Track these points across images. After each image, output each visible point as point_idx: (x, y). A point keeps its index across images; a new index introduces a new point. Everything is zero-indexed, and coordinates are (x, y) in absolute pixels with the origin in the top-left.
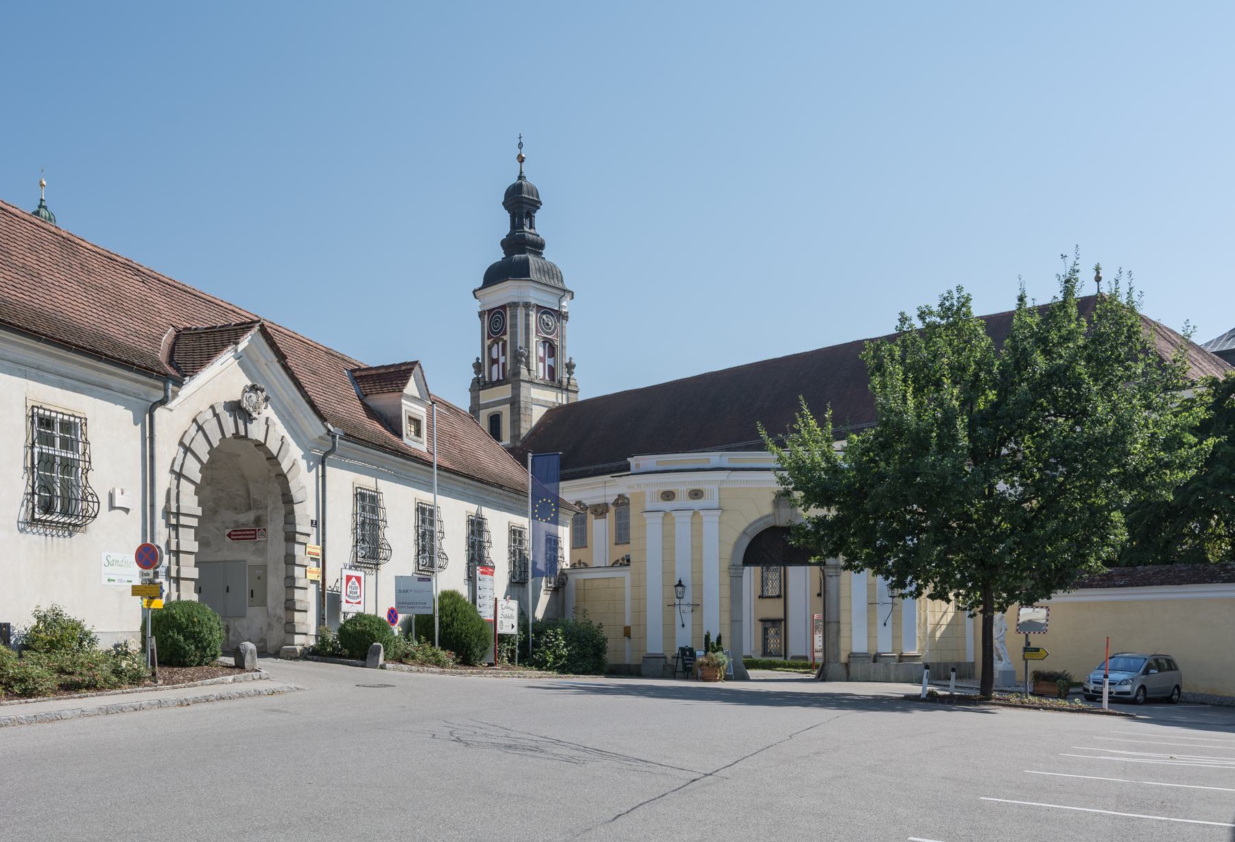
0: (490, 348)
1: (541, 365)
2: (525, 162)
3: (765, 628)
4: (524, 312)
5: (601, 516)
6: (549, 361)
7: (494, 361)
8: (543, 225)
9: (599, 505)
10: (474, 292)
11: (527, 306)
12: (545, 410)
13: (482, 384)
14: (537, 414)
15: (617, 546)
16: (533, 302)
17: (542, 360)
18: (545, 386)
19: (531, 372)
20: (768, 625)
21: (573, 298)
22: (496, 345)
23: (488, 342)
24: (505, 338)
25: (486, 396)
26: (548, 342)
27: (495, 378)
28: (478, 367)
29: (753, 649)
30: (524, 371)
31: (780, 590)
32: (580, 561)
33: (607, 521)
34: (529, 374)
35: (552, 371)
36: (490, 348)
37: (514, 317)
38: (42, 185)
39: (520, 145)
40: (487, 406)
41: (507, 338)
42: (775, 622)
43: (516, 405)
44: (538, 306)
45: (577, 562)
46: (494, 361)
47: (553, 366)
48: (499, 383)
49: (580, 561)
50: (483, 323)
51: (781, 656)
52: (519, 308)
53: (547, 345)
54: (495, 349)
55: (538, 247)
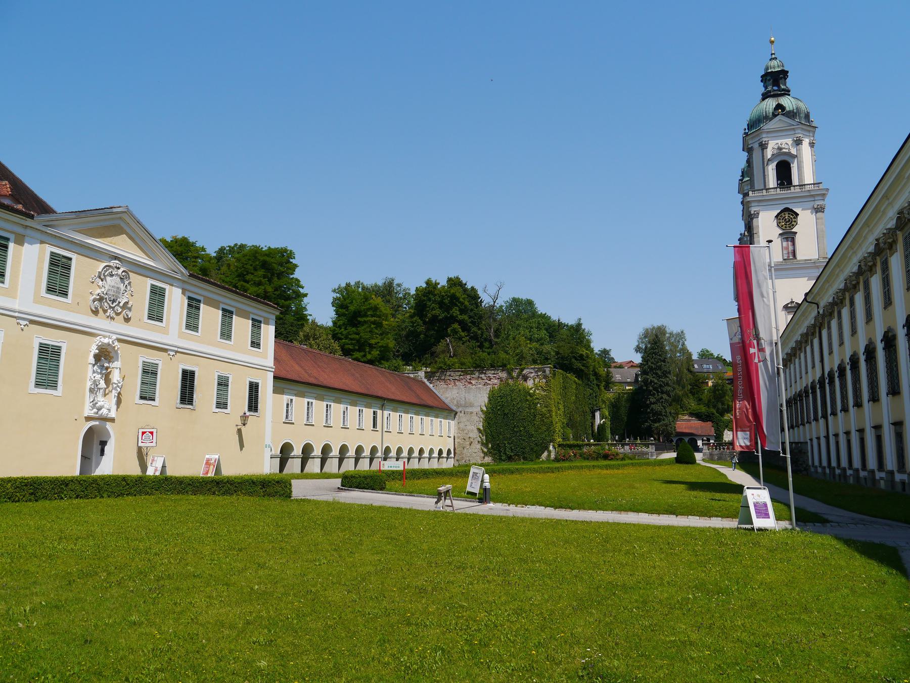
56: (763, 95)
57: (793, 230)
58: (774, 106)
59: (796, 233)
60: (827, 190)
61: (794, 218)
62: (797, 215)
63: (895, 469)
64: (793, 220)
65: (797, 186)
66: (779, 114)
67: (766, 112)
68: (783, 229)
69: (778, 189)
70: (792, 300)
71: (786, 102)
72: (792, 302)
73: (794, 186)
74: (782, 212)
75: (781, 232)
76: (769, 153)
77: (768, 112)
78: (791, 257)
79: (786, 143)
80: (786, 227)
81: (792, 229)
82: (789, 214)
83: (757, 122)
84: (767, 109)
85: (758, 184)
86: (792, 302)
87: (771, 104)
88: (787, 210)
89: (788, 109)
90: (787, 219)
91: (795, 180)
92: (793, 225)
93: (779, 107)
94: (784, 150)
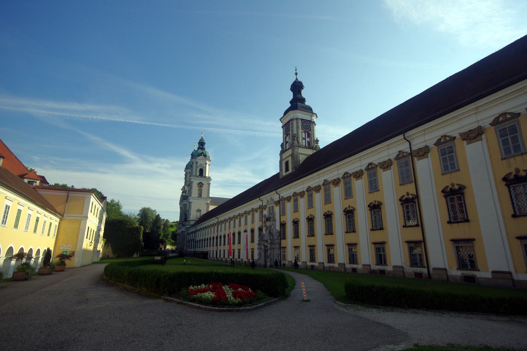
0: (286, 138)
1: (304, 141)
2: (298, 75)
3: (410, 247)
4: (296, 121)
5: (318, 192)
6: (307, 139)
7: (287, 142)
8: (304, 93)
9: (316, 186)
10: (280, 120)
11: (297, 119)
12: (306, 157)
13: (283, 151)
14: (302, 158)
15: (326, 205)
16: (299, 117)
17: (305, 139)
18: (305, 147)
19: (299, 143)
20: (412, 245)
21: (317, 117)
22: (288, 136)
23: (285, 136)
24: (289, 133)
25: (285, 155)
26: (307, 132)
27: (287, 148)
28: (282, 146)
29: (403, 261)
30: (296, 142)
31: (418, 221)
32: (311, 214)
33: (321, 194)
34: (298, 144)
35: (309, 143)
36: (286, 138)
37: (292, 124)
38: (202, 133)
39: (296, 70)
40: (285, 159)
41: (290, 132)
42: (417, 243)
43: (293, 156)
44: (301, 119)
45: (309, 215)
46: (287, 142)
47: (309, 141)
48: (289, 149)
49: (311, 214)
50: (283, 130)
51: (425, 267)
52: (294, 121)
53: (306, 133)
54: (287, 138)
55: (303, 100)
59: (202, 190)
60: (212, 179)
62: (203, 184)
63: (227, 258)
71: (204, 152)
72: (199, 209)
74: (200, 183)
75: (199, 188)
76: (198, 165)
79: (203, 163)
85: (194, 173)
86: (199, 209)
87: (200, 151)
88: (201, 183)
89: (204, 154)
90: (200, 185)
91: (204, 175)
93: (202, 153)
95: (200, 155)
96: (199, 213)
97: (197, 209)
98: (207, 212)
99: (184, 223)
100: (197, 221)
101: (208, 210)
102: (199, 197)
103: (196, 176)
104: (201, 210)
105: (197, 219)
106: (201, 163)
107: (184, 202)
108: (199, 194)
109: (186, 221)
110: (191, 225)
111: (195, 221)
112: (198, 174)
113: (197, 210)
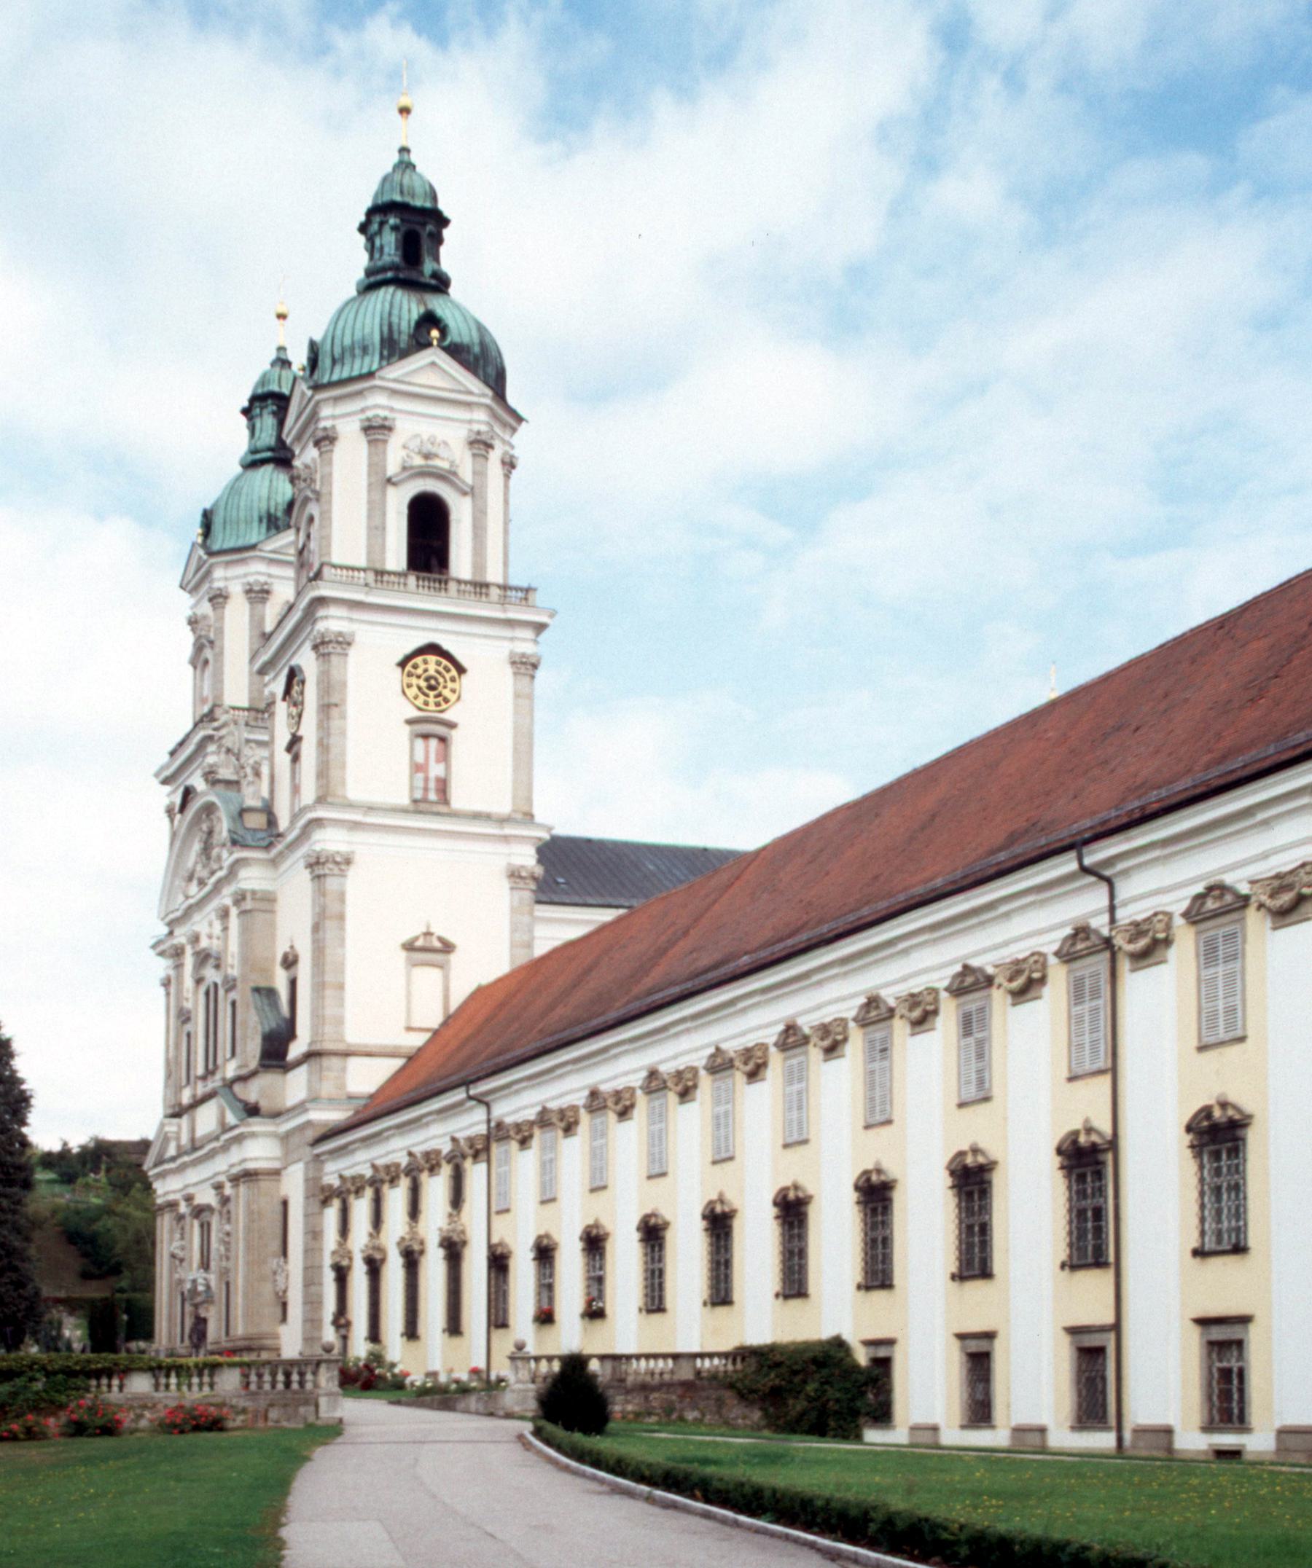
56: (369, 273)
57: (446, 716)
58: (415, 316)
59: (452, 726)
61: (453, 680)
62: (461, 670)
64: (450, 685)
65: (466, 583)
66: (429, 345)
67: (390, 325)
68: (420, 709)
69: (412, 580)
70: (428, 927)
72: (428, 934)
73: (459, 582)
75: (416, 714)
77: (395, 328)
78: (432, 796)
80: (426, 704)
81: (442, 711)
82: (439, 664)
83: (357, 351)
84: (395, 320)
86: (428, 934)
87: (408, 307)
88: (433, 649)
92: (446, 701)
94: (437, 463)
95: (404, 340)
96: (435, 974)
97: (412, 930)
98: (523, 959)
99: (251, 1092)
100: (412, 1058)
101: (529, 945)
102: (418, 806)
103: (380, 573)
104: (447, 947)
105: (418, 1040)
106: (426, 429)
107: (243, 873)
108: (417, 768)
109: (286, 1068)
110: (351, 1097)
111: (398, 1063)
112: (396, 554)
113: (409, 947)
